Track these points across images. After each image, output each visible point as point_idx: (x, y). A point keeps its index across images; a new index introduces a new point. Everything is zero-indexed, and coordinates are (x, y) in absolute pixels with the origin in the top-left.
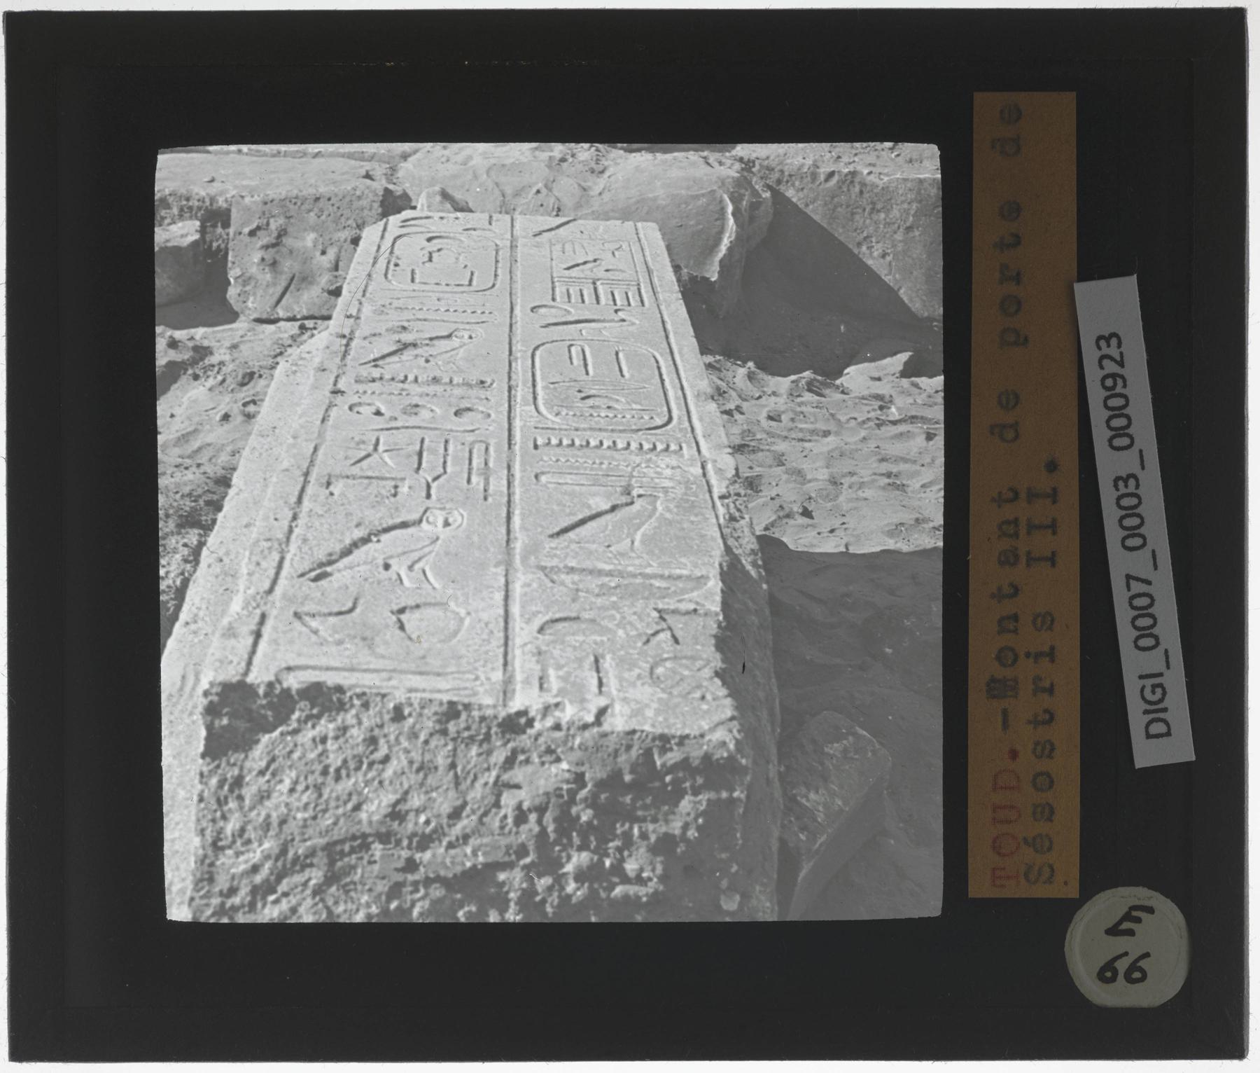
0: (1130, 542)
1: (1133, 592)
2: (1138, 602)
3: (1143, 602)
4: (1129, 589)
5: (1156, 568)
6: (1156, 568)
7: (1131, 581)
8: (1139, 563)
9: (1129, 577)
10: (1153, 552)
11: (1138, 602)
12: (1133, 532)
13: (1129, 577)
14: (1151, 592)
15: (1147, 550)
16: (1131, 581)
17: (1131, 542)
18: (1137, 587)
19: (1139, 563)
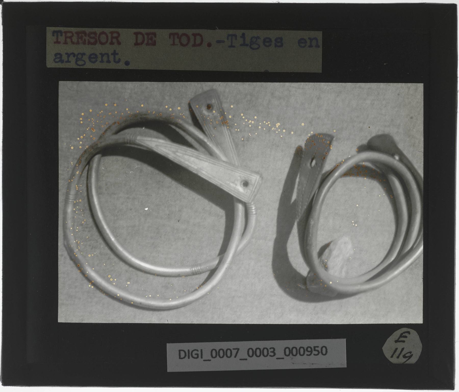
0: (251, 351)
1: (233, 351)
2: (229, 352)
3: (229, 355)
4: (234, 349)
5: (240, 359)
6: (240, 359)
7: (236, 350)
8: (243, 354)
9: (238, 349)
10: (246, 359)
11: (229, 352)
12: (254, 353)
13: (238, 349)
14: (232, 356)
15: (247, 357)
16: (236, 350)
17: (251, 351)
18: (234, 352)
19: (243, 354)
